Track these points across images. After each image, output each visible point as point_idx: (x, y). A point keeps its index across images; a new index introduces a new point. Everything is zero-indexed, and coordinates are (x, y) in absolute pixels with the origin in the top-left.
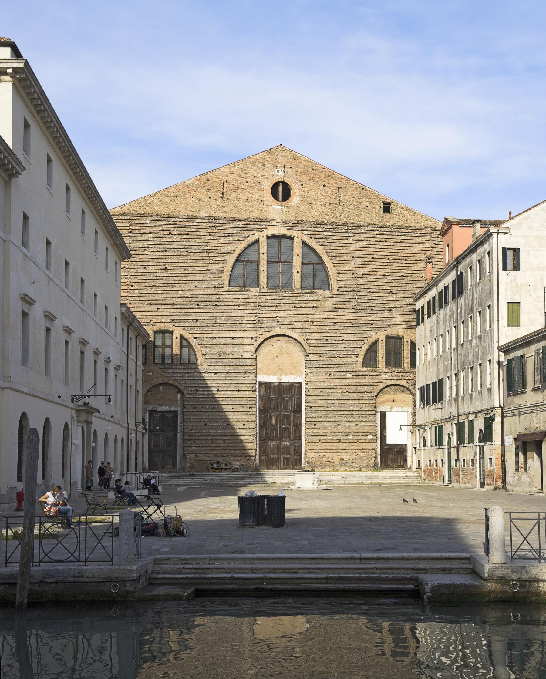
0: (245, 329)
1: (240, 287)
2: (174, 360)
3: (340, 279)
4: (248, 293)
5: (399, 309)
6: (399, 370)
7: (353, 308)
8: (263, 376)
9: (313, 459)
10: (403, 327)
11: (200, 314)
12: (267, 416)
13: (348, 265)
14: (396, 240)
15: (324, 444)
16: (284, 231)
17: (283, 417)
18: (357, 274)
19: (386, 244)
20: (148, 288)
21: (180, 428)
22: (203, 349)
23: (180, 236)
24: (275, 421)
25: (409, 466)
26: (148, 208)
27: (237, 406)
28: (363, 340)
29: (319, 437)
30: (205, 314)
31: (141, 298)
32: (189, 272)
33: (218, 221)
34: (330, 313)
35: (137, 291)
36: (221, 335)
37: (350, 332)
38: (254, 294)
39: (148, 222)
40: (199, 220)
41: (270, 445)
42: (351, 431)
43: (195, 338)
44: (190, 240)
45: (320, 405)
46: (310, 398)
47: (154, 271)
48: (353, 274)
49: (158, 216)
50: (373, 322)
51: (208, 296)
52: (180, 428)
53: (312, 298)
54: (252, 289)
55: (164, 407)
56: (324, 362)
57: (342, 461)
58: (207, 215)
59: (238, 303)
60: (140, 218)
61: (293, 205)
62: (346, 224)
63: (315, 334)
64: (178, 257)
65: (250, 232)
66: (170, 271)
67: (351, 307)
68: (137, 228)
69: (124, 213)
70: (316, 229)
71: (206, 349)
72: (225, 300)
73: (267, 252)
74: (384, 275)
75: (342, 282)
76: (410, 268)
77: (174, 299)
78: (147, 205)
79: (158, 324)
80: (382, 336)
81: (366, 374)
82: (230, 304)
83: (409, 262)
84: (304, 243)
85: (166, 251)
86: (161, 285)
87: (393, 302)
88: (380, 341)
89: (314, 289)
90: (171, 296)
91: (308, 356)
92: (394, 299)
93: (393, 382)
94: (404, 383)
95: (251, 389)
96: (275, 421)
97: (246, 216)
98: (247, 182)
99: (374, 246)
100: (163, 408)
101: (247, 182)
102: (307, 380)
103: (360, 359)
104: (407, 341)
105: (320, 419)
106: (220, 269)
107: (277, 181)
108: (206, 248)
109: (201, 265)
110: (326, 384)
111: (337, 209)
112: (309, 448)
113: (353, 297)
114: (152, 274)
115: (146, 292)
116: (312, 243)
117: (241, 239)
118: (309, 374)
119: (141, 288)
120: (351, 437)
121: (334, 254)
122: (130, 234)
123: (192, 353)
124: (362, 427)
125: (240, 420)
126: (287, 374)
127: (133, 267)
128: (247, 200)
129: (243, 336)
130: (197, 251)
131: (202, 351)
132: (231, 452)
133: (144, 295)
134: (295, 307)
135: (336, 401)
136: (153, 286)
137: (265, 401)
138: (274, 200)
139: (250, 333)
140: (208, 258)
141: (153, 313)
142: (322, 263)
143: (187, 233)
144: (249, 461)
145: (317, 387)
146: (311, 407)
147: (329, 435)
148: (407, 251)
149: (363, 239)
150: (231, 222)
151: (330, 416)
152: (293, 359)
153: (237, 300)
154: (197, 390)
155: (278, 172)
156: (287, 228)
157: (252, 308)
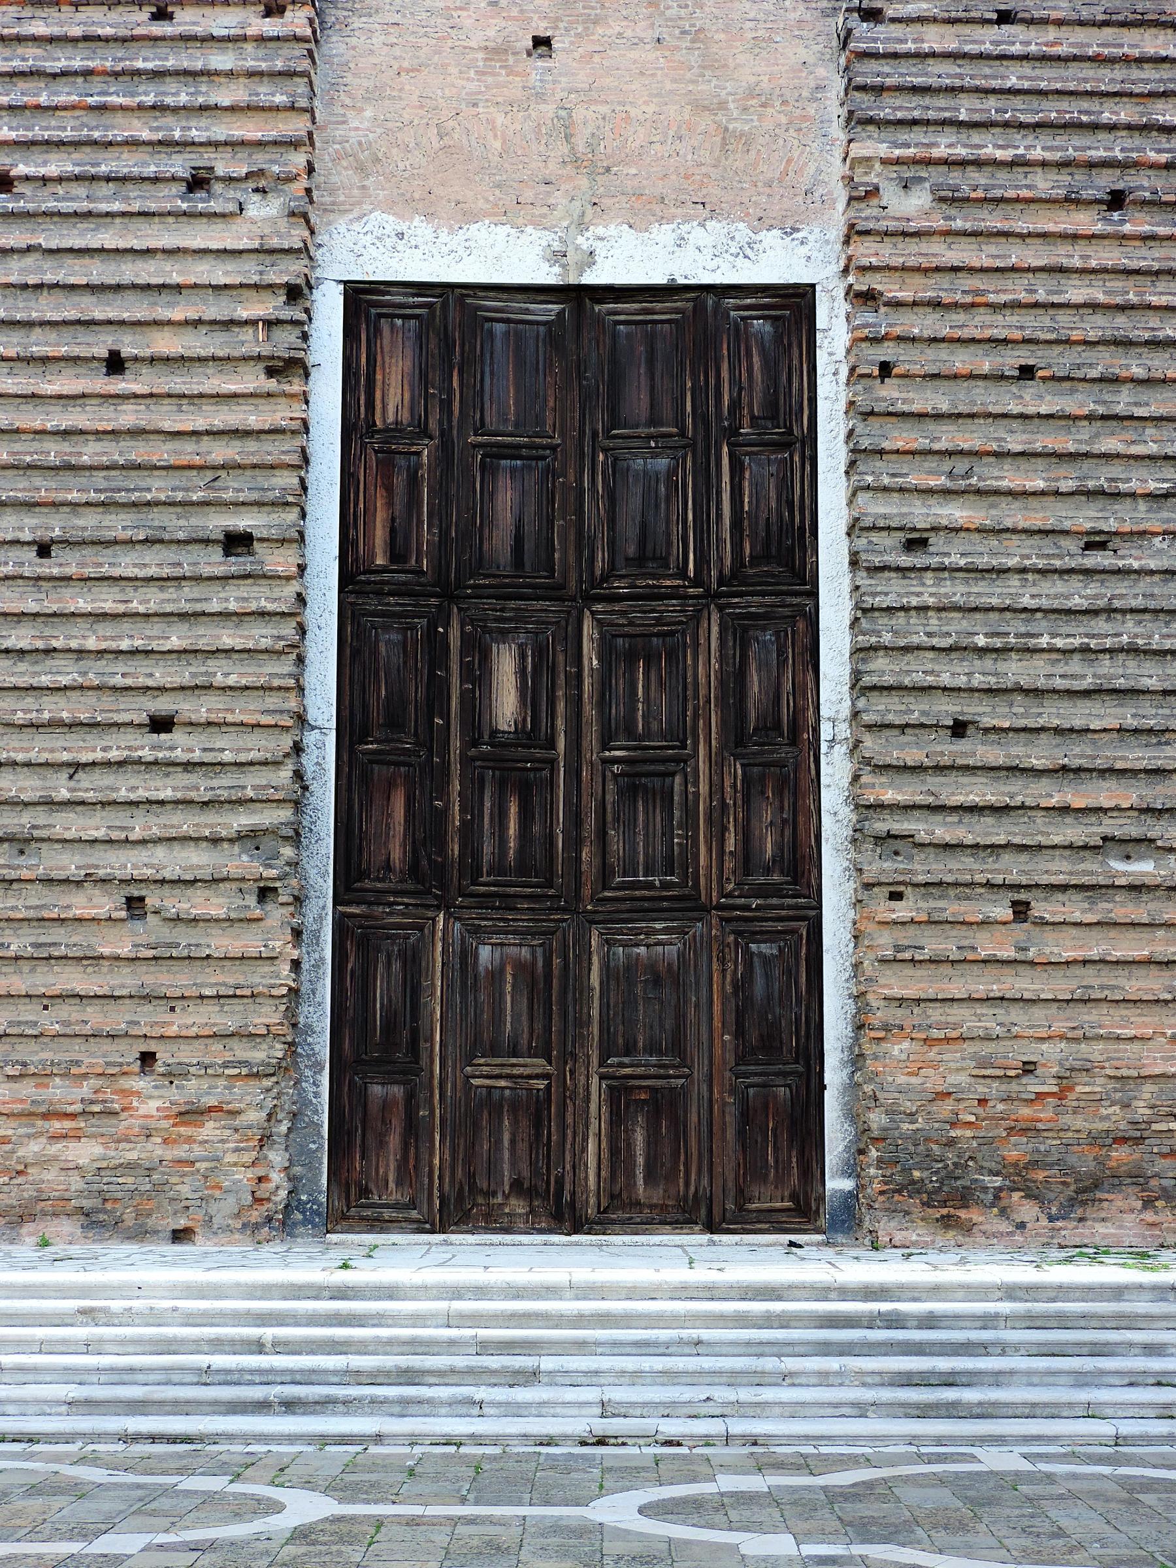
8: (392, 223)
9: (945, 1109)
12: (437, 649)
15: (1065, 947)
17: (606, 651)
24: (529, 696)
27: (88, 523)
29: (1013, 868)
41: (467, 957)
45: (1015, 515)
46: (900, 437)
56: (1048, 77)
95: (251, 342)
96: (522, 690)
102: (867, 251)
105: (1015, 671)
110: (1077, 292)
112: (898, 983)
125: (118, 673)
137: (413, 481)
144: (210, 1129)
145: (978, 324)
146: (917, 543)
147: (1130, 846)
151: (1129, 631)
152: (713, 66)
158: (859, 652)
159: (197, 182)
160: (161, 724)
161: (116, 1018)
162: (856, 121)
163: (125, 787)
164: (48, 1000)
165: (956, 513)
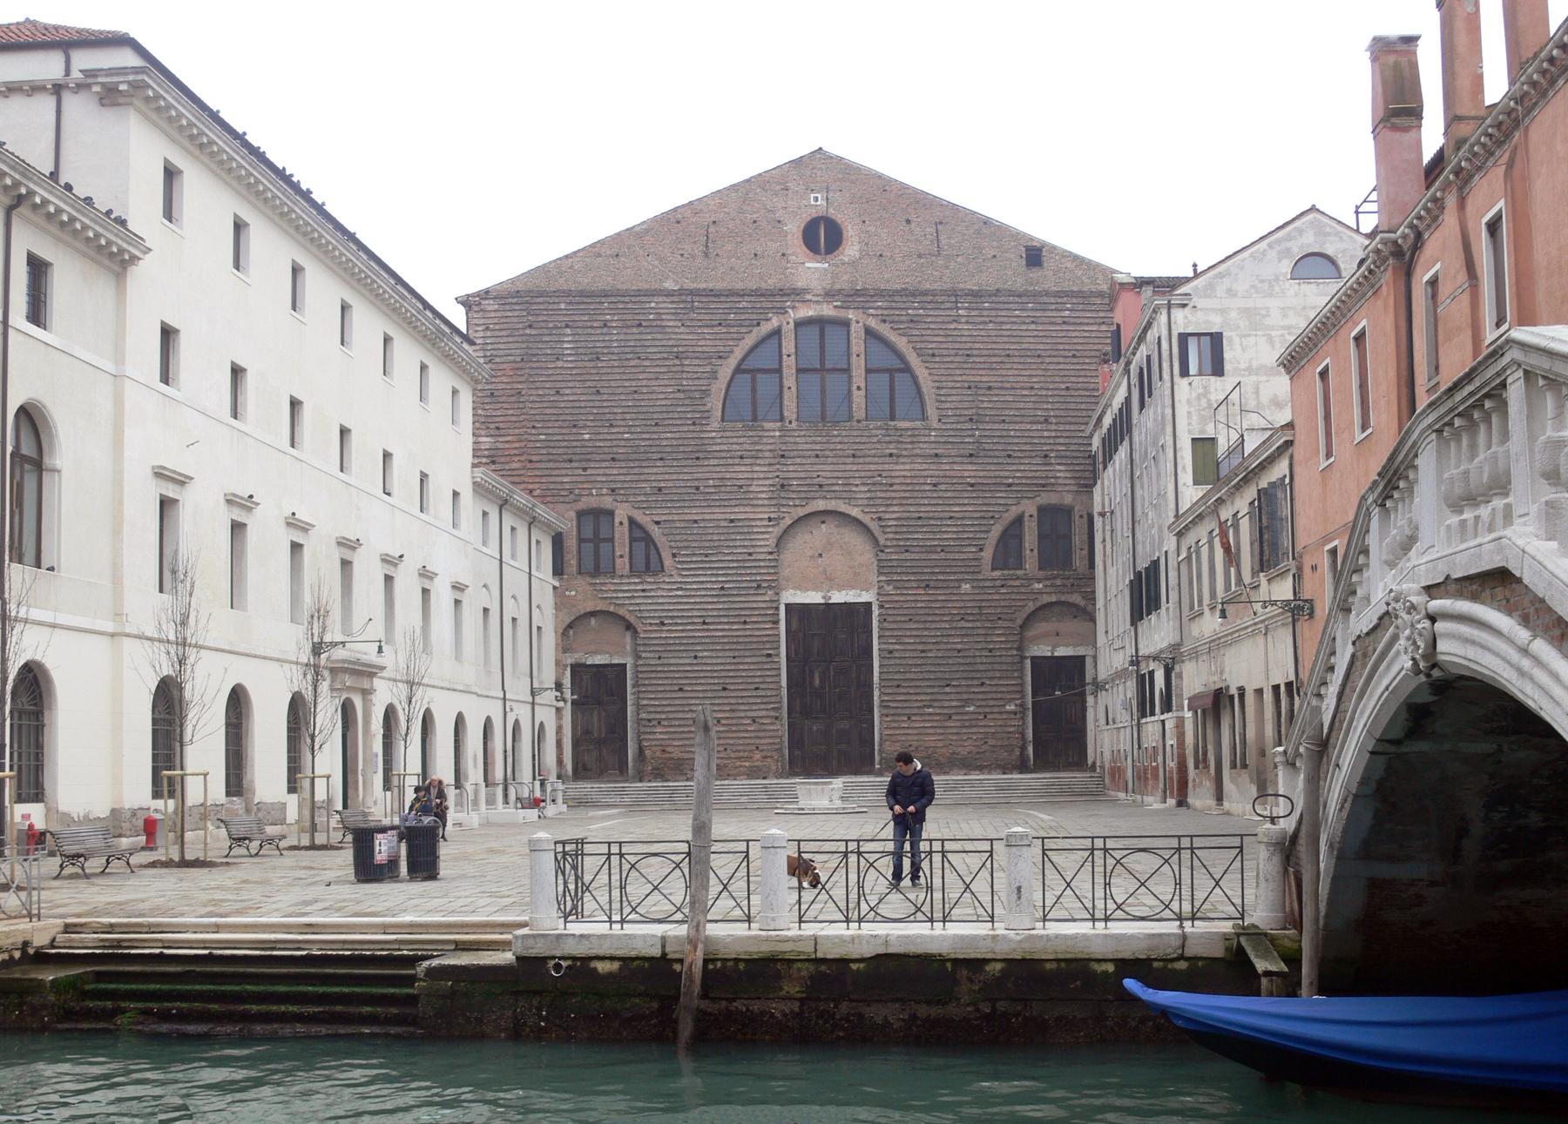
0: (755, 502)
1: (743, 421)
2: (617, 567)
3: (943, 399)
4: (760, 434)
5: (1063, 453)
6: (1067, 573)
7: (971, 455)
10: (1072, 488)
11: (667, 477)
12: (804, 672)
13: (958, 372)
14: (1053, 320)
16: (827, 310)
18: (976, 387)
19: (1033, 327)
20: (564, 431)
21: (633, 697)
22: (673, 544)
23: (625, 330)
24: (821, 681)
25: (1090, 762)
26: (562, 281)
28: (993, 517)
29: (908, 711)
30: (675, 477)
31: (551, 450)
32: (642, 397)
33: (697, 299)
34: (925, 466)
35: (543, 437)
36: (707, 517)
37: (966, 501)
38: (772, 434)
39: (563, 306)
40: (660, 299)
41: (811, 729)
42: (972, 696)
43: (657, 523)
44: (644, 337)
47: (575, 398)
48: (969, 388)
49: (582, 294)
50: (1011, 480)
51: (680, 442)
52: (633, 697)
53: (888, 438)
54: (767, 425)
55: (599, 657)
57: (955, 756)
58: (676, 288)
59: (740, 453)
60: (548, 299)
61: (846, 259)
62: (954, 293)
63: (896, 509)
64: (621, 370)
65: (762, 317)
66: (605, 397)
67: (967, 452)
68: (541, 318)
69: (518, 292)
70: (893, 304)
71: (680, 544)
72: (715, 448)
73: (796, 352)
74: (1032, 388)
75: (948, 405)
76: (1082, 373)
77: (615, 450)
78: (561, 274)
79: (583, 499)
80: (1030, 508)
81: (998, 583)
82: (724, 454)
83: (1081, 360)
84: (869, 332)
85: (598, 359)
86: (589, 423)
87: (1051, 441)
88: (1026, 518)
89: (893, 418)
90: (609, 444)
91: (882, 551)
92: (1053, 434)
93: (1054, 599)
94: (1076, 598)
97: (753, 285)
98: (755, 222)
99: (1009, 333)
100: (599, 660)
101: (755, 222)
103: (987, 555)
104: (1081, 516)
105: (908, 676)
106: (704, 388)
107: (815, 216)
108: (675, 350)
109: (666, 382)
111: (935, 264)
113: (970, 433)
114: (570, 404)
115: (560, 438)
116: (885, 330)
117: (743, 329)
118: (886, 586)
119: (550, 431)
120: (972, 709)
121: (931, 352)
122: (528, 331)
123: (653, 552)
124: (994, 689)
126: (840, 588)
127: (534, 392)
128: (756, 255)
129: (752, 516)
130: (659, 356)
131: (671, 547)
132: (731, 742)
133: (557, 444)
134: (854, 456)
135: (939, 639)
136: (575, 426)
138: (808, 252)
139: (766, 509)
140: (680, 368)
141: (574, 479)
142: (907, 369)
143: (637, 322)
144: (769, 760)
147: (929, 707)
148: (1075, 341)
149: (987, 319)
150: (722, 299)
151: (929, 668)
153: (738, 447)
154: (663, 624)
155: (816, 199)
156: (835, 304)
157: (767, 461)
158: (880, 673)
159: (759, 587)
160: (757, 689)
161: (753, 742)
162: (880, 574)
163: (751, 700)
164: (739, 738)
165: (897, 647)
